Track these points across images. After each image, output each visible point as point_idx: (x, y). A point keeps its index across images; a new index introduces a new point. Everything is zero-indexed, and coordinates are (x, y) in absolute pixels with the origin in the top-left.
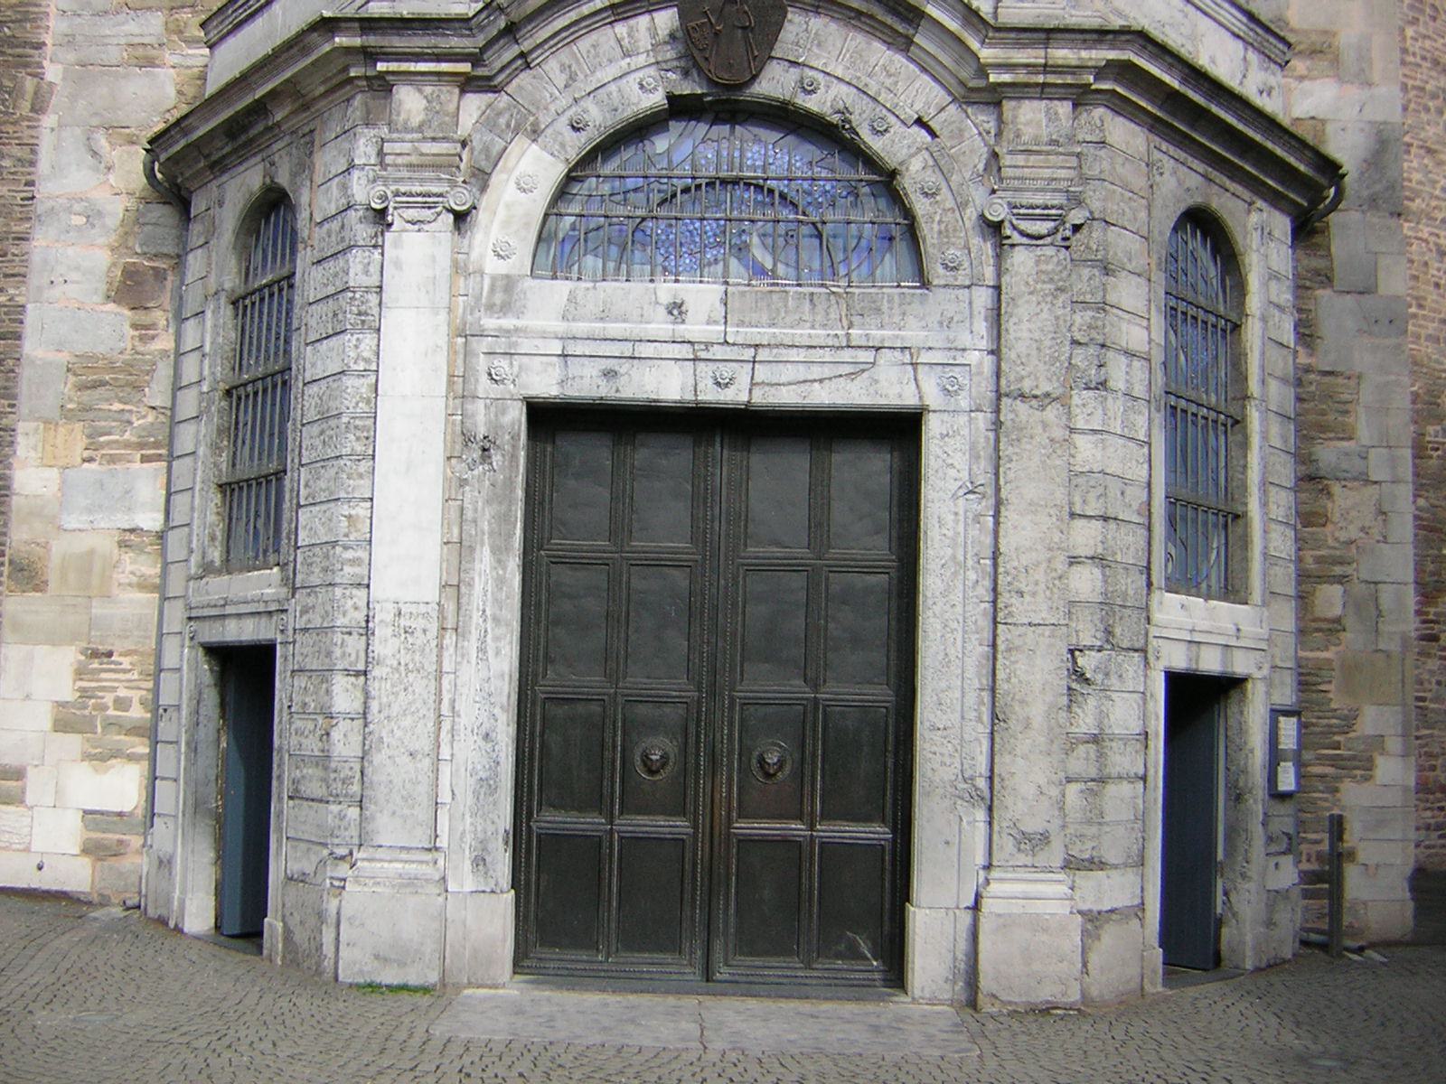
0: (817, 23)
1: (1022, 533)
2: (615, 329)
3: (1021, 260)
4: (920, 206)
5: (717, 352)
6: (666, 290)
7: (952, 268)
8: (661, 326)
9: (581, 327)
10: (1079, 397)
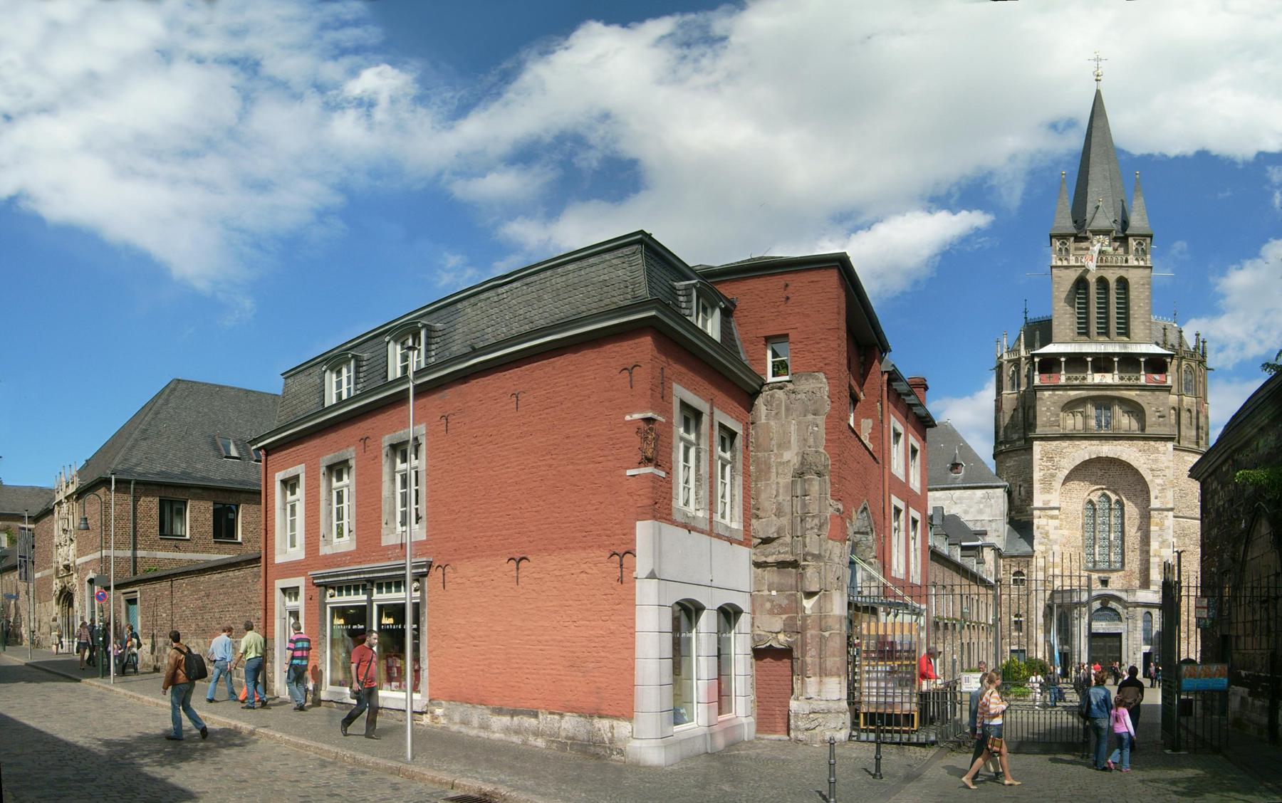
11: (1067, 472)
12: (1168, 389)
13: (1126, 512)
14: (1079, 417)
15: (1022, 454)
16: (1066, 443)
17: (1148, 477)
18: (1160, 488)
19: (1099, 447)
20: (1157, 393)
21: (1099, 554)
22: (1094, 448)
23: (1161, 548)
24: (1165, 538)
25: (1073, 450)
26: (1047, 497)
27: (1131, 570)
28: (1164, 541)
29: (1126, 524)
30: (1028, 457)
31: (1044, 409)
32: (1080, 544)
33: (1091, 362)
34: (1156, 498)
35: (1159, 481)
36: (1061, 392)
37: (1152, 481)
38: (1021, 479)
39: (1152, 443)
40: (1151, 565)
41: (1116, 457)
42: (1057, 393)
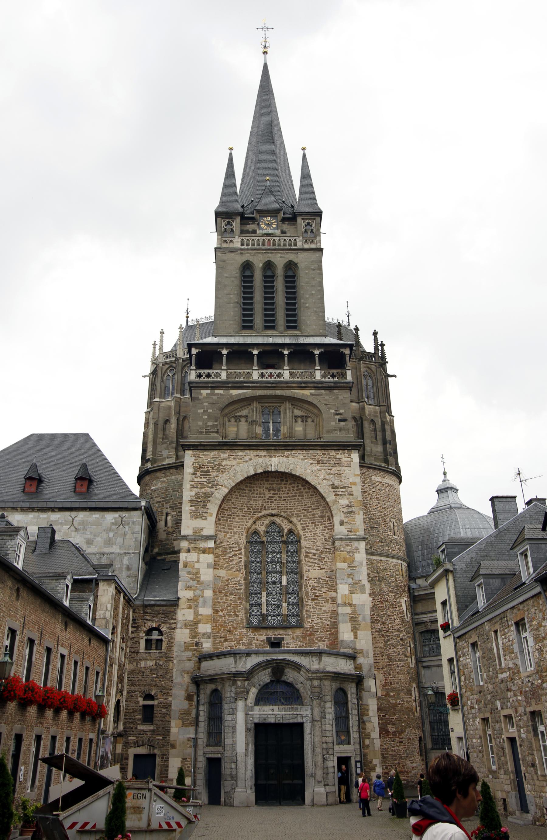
0: (288, 670)
1: (317, 739)
2: (265, 713)
3: (315, 702)
4: (302, 694)
5: (278, 716)
6: (271, 707)
7: (306, 703)
8: (271, 713)
9: (261, 713)
10: (323, 720)
11: (227, 491)
12: (348, 387)
13: (303, 546)
14: (243, 425)
15: (172, 474)
16: (224, 455)
17: (330, 498)
18: (345, 510)
19: (267, 460)
20: (336, 391)
21: (268, 604)
22: (260, 460)
23: (352, 593)
24: (356, 578)
25: (234, 463)
26: (199, 523)
27: (312, 627)
28: (355, 584)
29: (303, 562)
30: (179, 477)
31: (200, 411)
32: (243, 590)
33: (258, 355)
34: (342, 523)
35: (344, 501)
36: (221, 391)
37: (336, 502)
38: (168, 505)
39: (333, 453)
40: (340, 618)
41: (288, 471)
42: (217, 391)
